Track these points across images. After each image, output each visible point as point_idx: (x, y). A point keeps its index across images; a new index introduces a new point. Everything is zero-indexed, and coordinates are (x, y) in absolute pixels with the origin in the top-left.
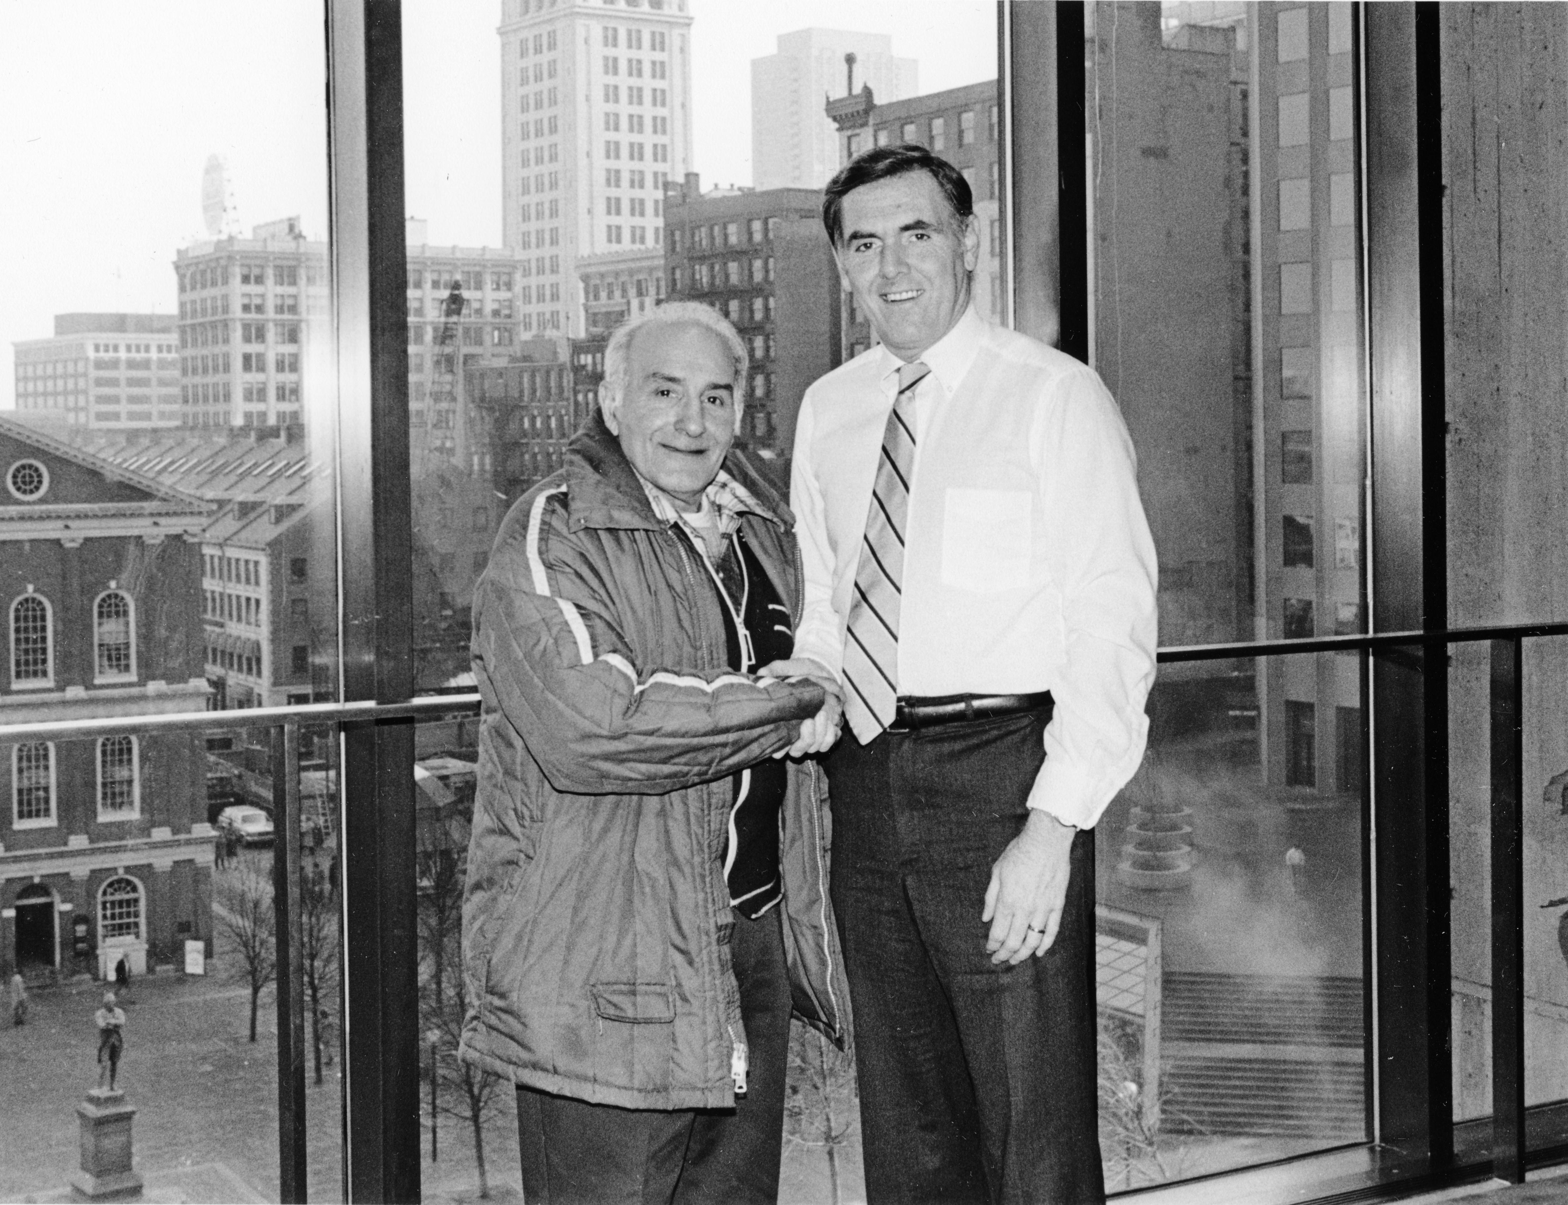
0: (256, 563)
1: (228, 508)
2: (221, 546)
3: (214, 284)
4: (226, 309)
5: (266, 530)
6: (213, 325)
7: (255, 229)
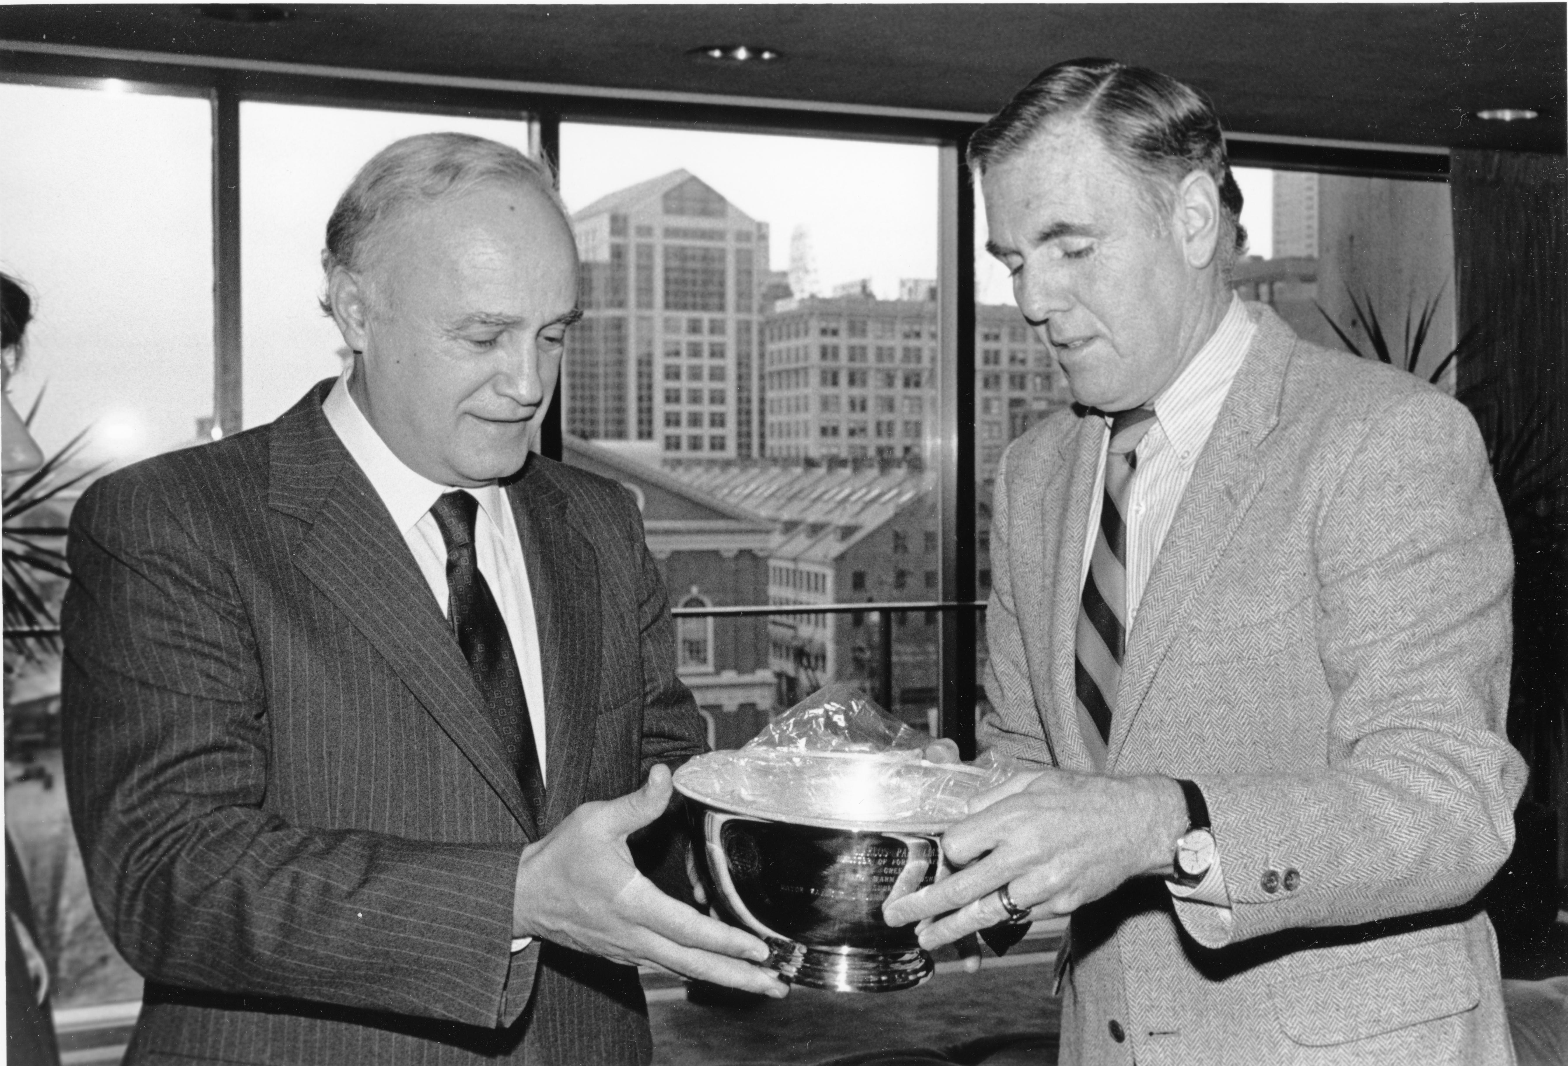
0: (824, 577)
1: (801, 527)
2: (795, 560)
3: (797, 335)
4: (806, 357)
5: (834, 547)
6: (797, 371)
7: (835, 289)
